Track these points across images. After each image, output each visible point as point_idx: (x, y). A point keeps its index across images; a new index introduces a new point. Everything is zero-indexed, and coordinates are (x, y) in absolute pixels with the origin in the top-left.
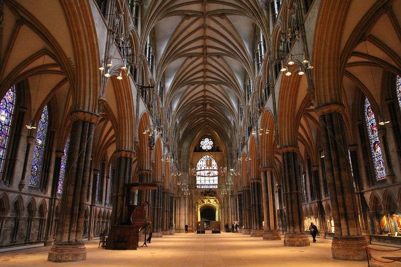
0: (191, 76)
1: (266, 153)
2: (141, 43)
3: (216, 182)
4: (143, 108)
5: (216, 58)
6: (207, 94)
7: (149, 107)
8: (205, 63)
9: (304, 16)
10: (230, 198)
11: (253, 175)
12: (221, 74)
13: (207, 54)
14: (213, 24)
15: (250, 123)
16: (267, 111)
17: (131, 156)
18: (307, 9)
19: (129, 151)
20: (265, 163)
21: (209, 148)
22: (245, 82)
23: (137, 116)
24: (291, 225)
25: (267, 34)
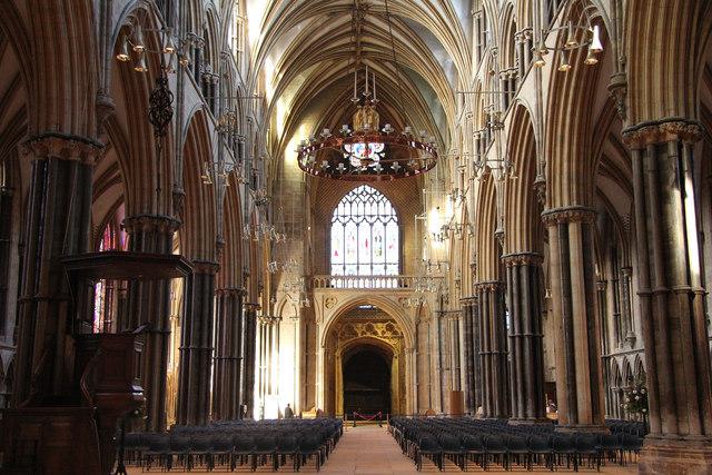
1: (569, 161)
3: (393, 270)
10: (435, 321)
11: (516, 245)
15: (511, 64)
17: (84, 155)
19: (76, 139)
24: (665, 411)
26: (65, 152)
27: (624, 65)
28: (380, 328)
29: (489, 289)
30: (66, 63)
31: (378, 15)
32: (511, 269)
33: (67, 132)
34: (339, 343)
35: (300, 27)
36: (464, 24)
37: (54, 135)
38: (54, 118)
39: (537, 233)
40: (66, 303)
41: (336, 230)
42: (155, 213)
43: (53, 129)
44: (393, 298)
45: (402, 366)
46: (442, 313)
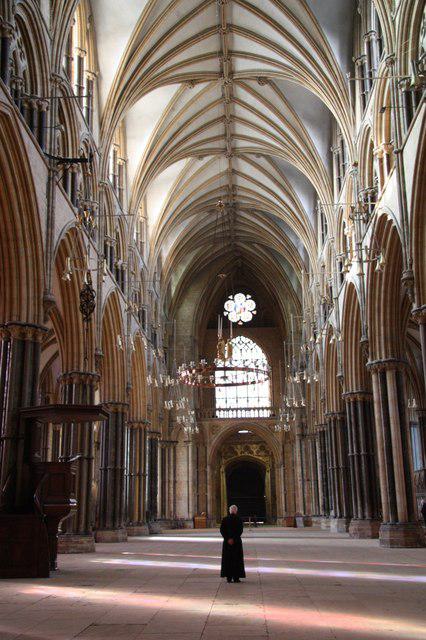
2: (53, 41)
5: (254, 84)
6: (241, 182)
10: (297, 443)
11: (353, 386)
13: (232, 73)
17: (35, 336)
21: (247, 317)
22: (330, 144)
23: (50, 235)
25: (387, 6)
26: (23, 335)
27: (411, 265)
28: (255, 448)
29: (335, 419)
30: (24, 274)
31: (247, 211)
32: (349, 403)
33: (24, 321)
34: (224, 461)
35: (188, 221)
36: (310, 217)
37: (16, 324)
38: (15, 312)
39: (365, 377)
40: (22, 441)
42: (82, 370)
43: (15, 319)
44: (264, 425)
45: (273, 478)
46: (303, 436)
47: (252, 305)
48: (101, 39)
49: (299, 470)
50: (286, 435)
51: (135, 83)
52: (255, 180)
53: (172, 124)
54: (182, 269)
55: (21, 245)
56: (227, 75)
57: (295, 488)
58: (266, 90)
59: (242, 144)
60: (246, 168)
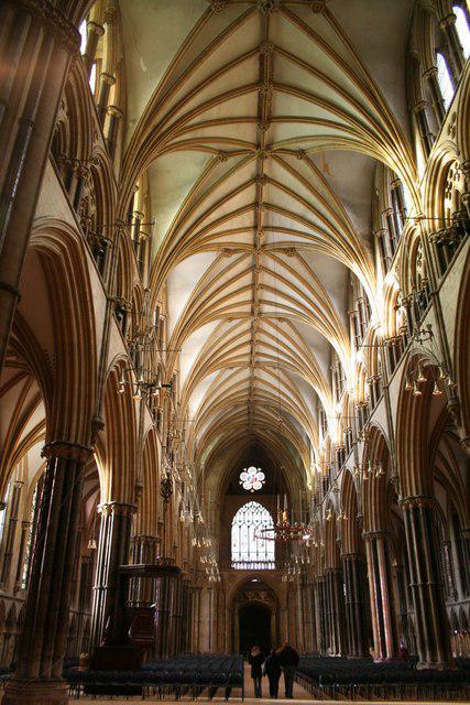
0: (230, 352)
3: (272, 557)
4: (149, 423)
5: (274, 321)
6: (260, 385)
7: (156, 416)
8: (254, 330)
9: (439, 281)
10: (299, 592)
11: (348, 548)
12: (281, 348)
13: (260, 313)
14: (271, 264)
16: (374, 428)
18: (444, 269)
20: (372, 527)
21: (258, 486)
31: (264, 406)
41: (235, 530)
46: (303, 586)
47: (261, 476)
48: (171, 292)
49: (300, 614)
50: (290, 584)
51: (190, 322)
52: (269, 381)
53: (216, 344)
54: (210, 448)
55: (123, 447)
56: (255, 313)
57: (297, 630)
58: (284, 326)
59: (263, 359)
60: (265, 376)
